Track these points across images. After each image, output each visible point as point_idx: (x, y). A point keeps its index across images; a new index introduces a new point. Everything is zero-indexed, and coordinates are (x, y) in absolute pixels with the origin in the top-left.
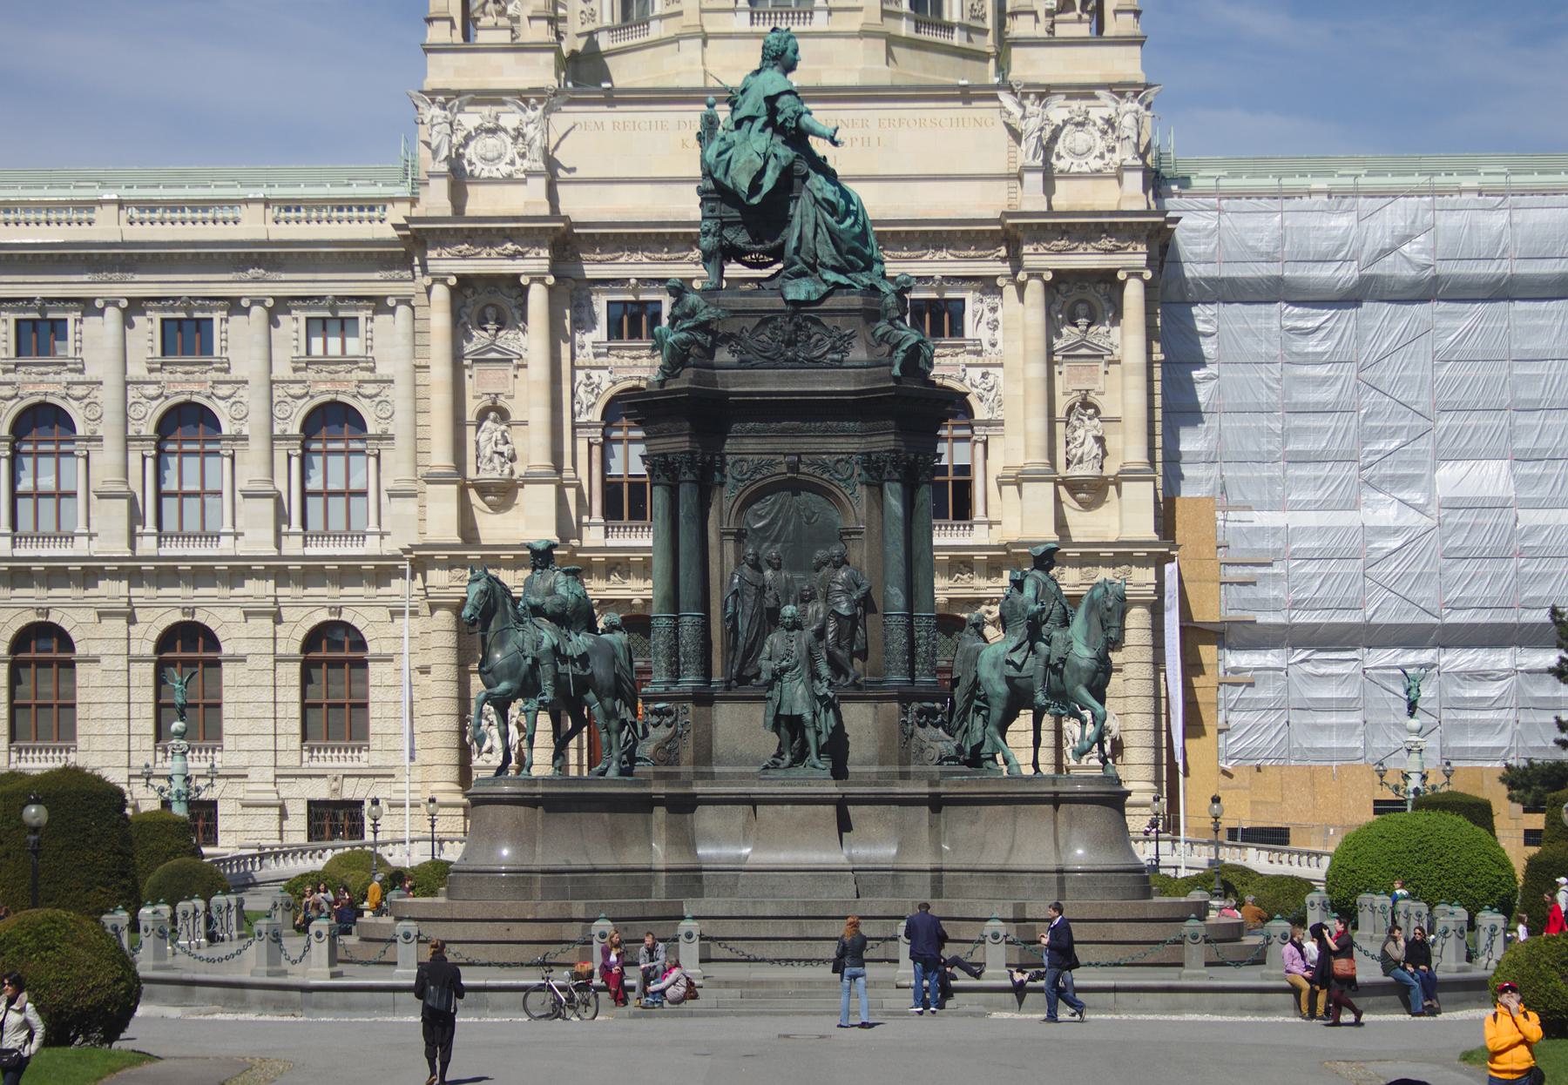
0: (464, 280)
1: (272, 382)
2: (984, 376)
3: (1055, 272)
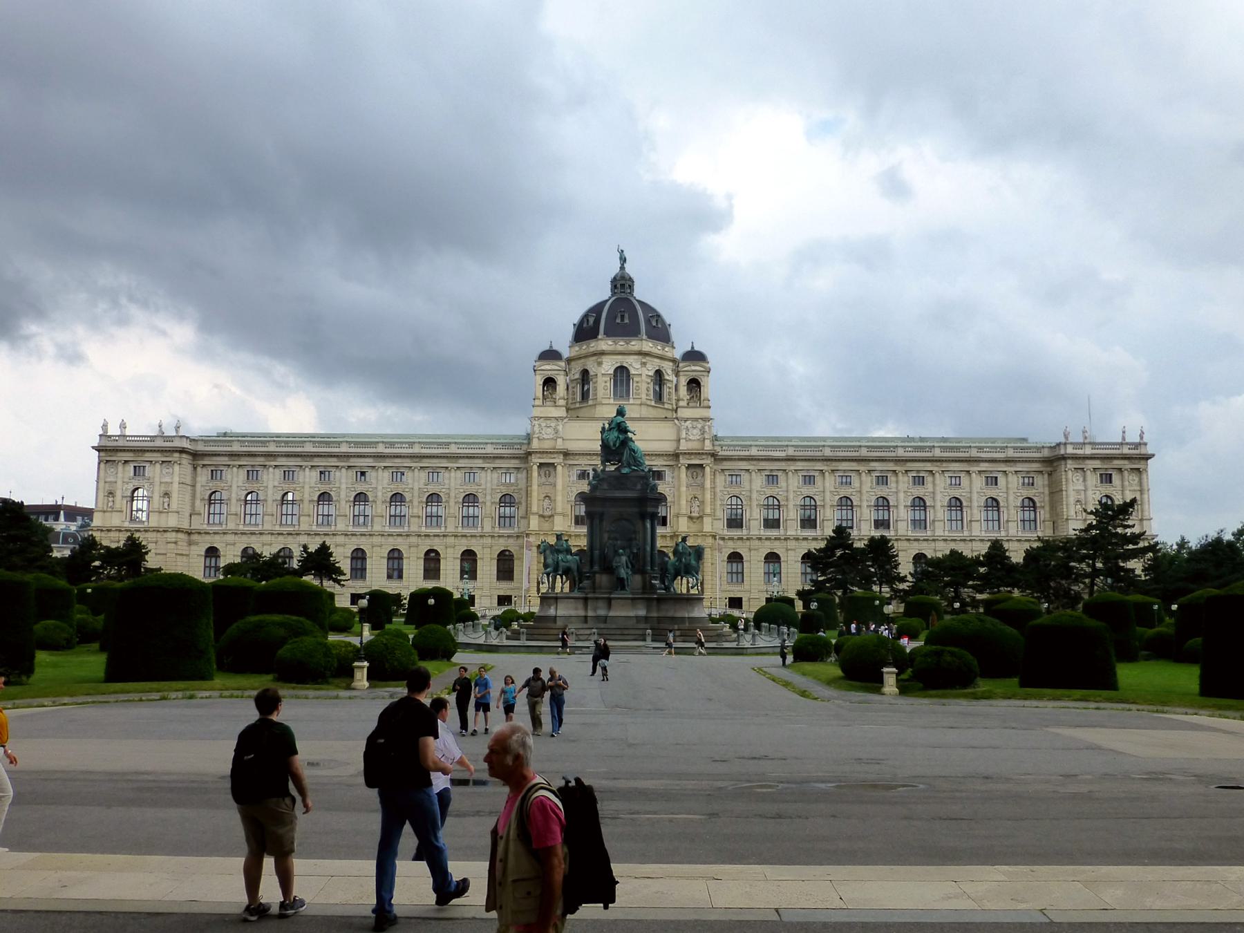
0: (541, 464)
2: (670, 490)
3: (688, 464)
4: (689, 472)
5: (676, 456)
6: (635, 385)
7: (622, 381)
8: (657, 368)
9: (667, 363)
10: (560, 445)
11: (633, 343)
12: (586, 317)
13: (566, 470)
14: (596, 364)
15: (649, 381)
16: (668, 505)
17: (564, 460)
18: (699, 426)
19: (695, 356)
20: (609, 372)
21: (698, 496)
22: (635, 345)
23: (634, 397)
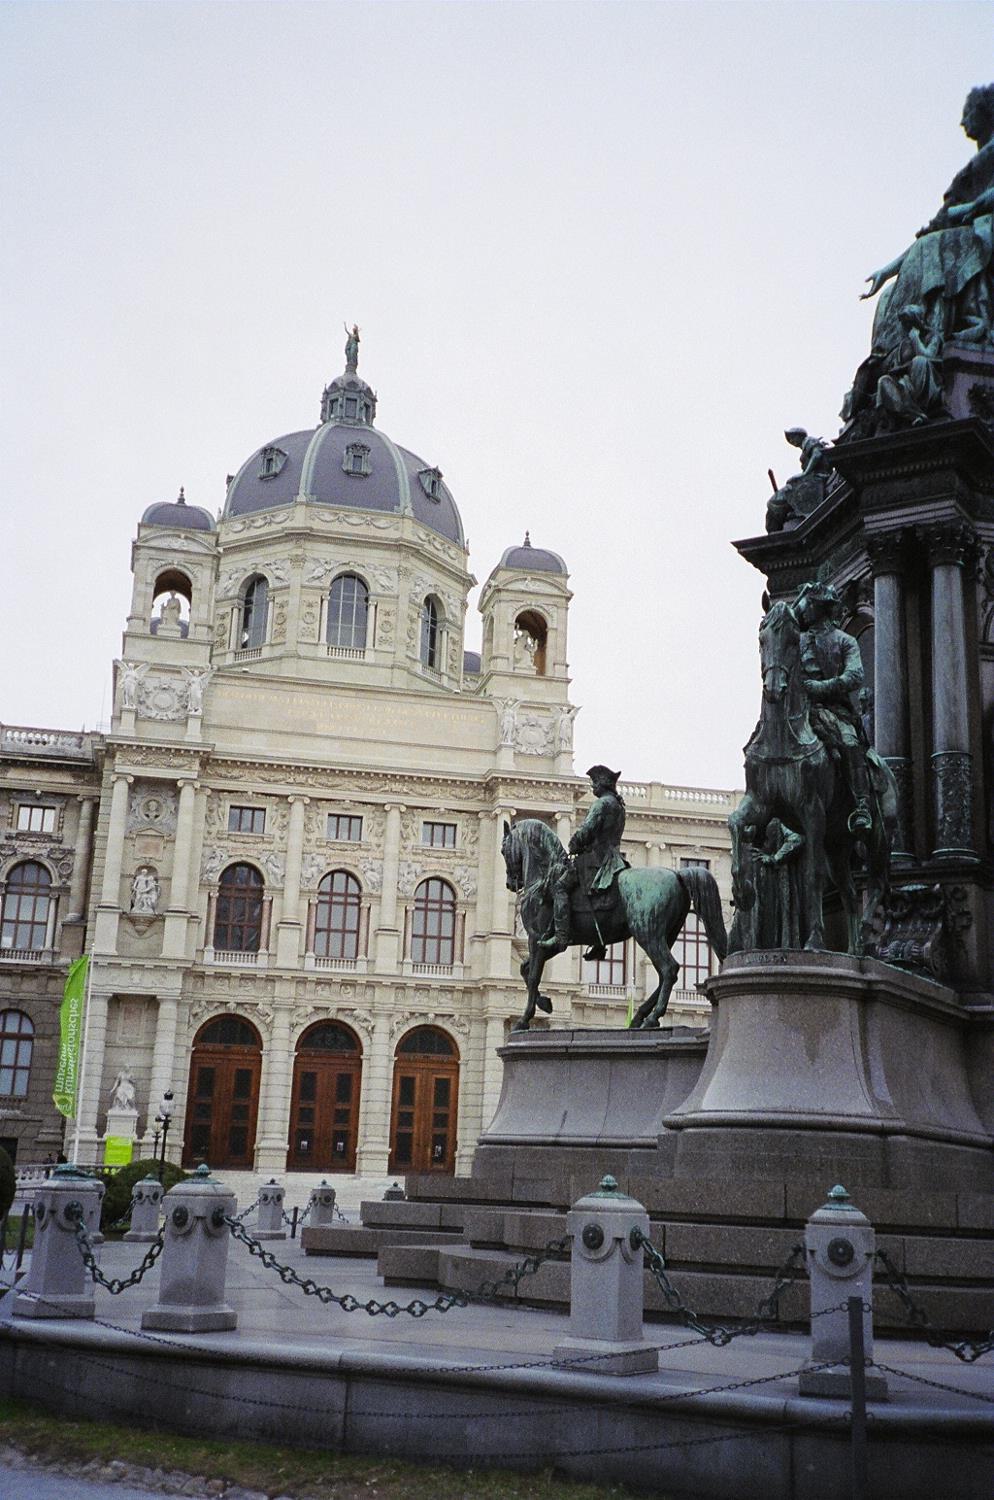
0: (139, 780)
3: (517, 810)
5: (489, 787)
6: (381, 618)
8: (432, 591)
10: (193, 735)
11: (382, 523)
12: (269, 453)
14: (288, 565)
15: (415, 616)
18: (545, 723)
19: (531, 561)
22: (386, 527)
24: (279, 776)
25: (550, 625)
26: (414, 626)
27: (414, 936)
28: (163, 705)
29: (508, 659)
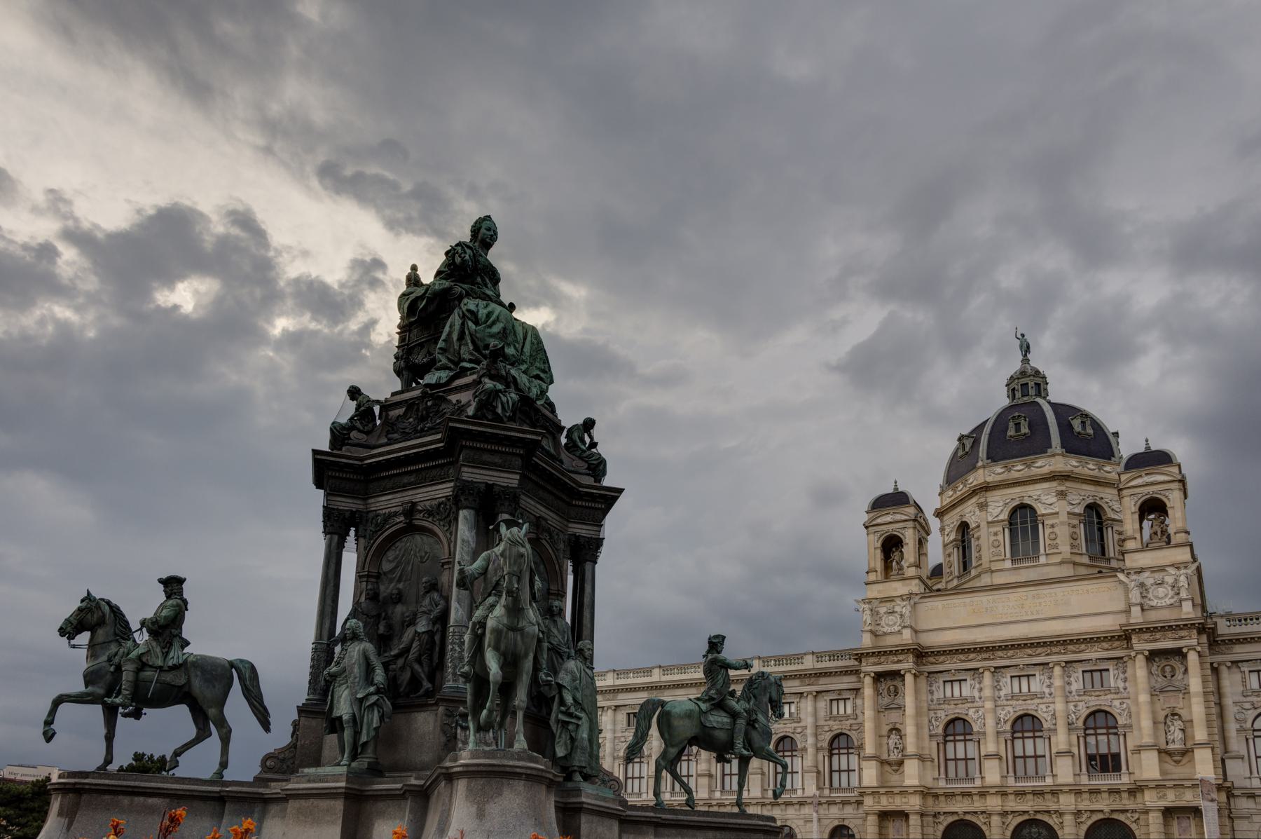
1: (817, 726)
2: (1121, 704)
4: (1154, 669)
5: (1126, 636)
6: (1048, 531)
7: (1025, 530)
9: (1108, 490)
13: (923, 681)
15: (1076, 522)
16: (1121, 731)
17: (916, 663)
20: (1001, 517)
21: (1180, 712)
23: (1047, 552)
24: (972, 656)
25: (1168, 504)
26: (1077, 530)
27: (1044, 756)
28: (891, 623)
29: (1135, 538)
